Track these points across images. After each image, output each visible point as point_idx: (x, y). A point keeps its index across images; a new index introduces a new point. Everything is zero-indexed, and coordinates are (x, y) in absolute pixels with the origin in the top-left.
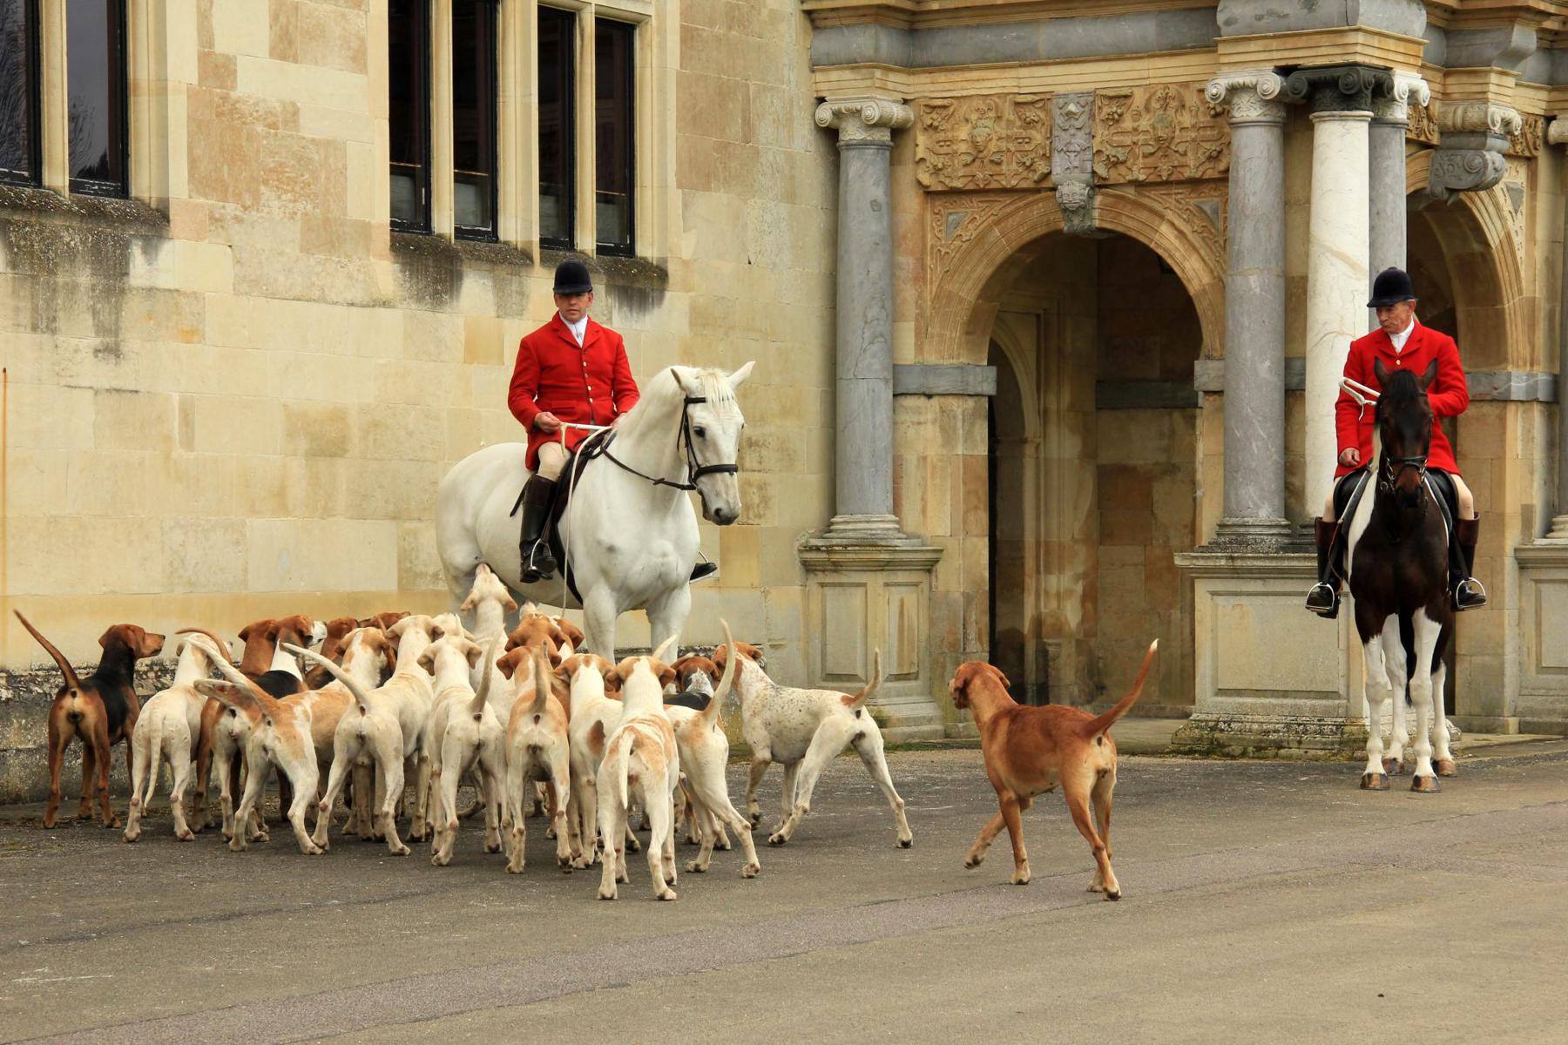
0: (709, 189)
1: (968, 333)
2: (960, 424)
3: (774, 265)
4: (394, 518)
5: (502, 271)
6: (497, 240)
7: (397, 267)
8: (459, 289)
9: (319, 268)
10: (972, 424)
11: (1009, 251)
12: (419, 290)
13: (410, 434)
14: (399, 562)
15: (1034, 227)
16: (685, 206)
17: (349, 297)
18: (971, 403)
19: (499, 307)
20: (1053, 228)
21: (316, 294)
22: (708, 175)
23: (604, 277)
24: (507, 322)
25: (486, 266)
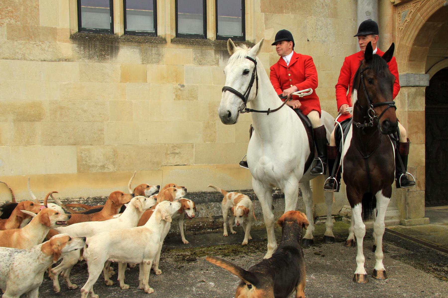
0: (282, 12)
1: (410, 60)
2: (407, 99)
3: (324, 42)
4: (74, 145)
5: (146, 46)
6: (157, 36)
7: (75, 45)
8: (116, 54)
9: (21, 46)
10: (415, 98)
11: (424, 22)
12: (89, 54)
13: (85, 111)
14: (78, 162)
15: (433, 8)
16: (267, 19)
17: (42, 58)
18: (413, 90)
19: (143, 60)
20: (441, 6)
21: (20, 57)
22: (282, 7)
23: (214, 48)
24: (149, 66)
25: (136, 44)
